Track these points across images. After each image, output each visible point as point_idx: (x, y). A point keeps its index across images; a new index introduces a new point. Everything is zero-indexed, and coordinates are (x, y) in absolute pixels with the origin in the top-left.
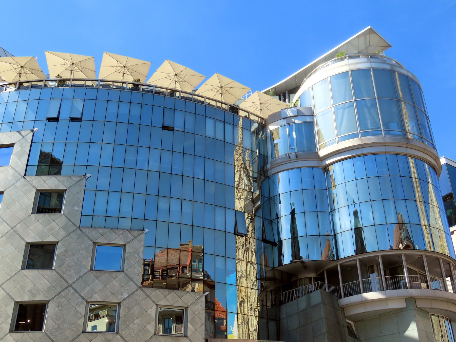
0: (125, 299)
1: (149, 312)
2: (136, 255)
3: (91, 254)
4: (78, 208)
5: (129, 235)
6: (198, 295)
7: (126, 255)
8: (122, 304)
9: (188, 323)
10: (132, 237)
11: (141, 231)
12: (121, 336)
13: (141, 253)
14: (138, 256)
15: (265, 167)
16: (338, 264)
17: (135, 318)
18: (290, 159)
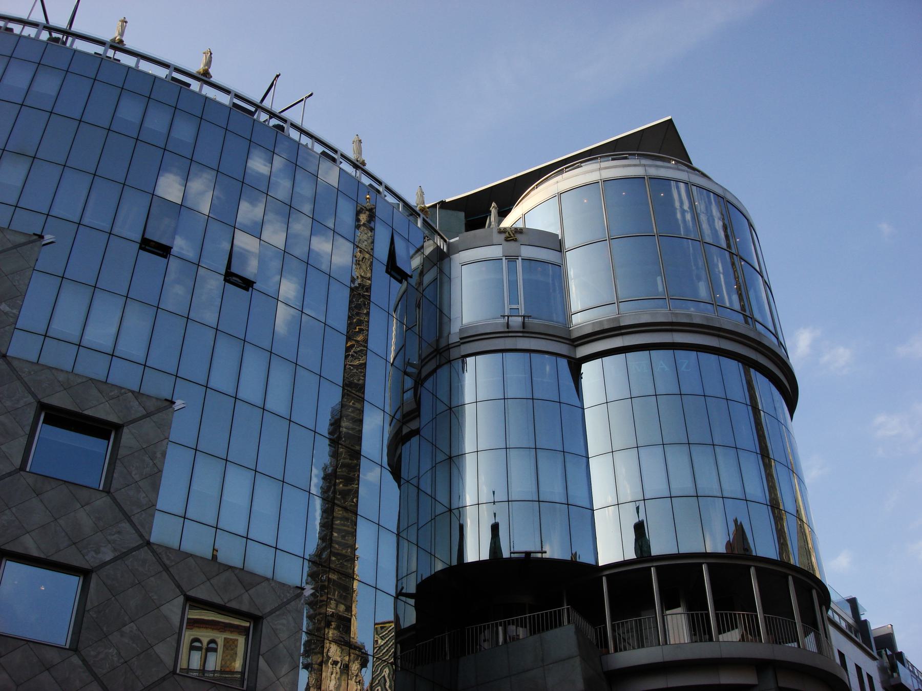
0: (104, 564)
1: (165, 609)
2: (147, 459)
3: (28, 429)
4: (10, 308)
5: (135, 404)
6: (289, 593)
7: (122, 452)
8: (94, 576)
9: (261, 658)
10: (141, 412)
14: (150, 461)
16: (604, 576)
17: (126, 618)
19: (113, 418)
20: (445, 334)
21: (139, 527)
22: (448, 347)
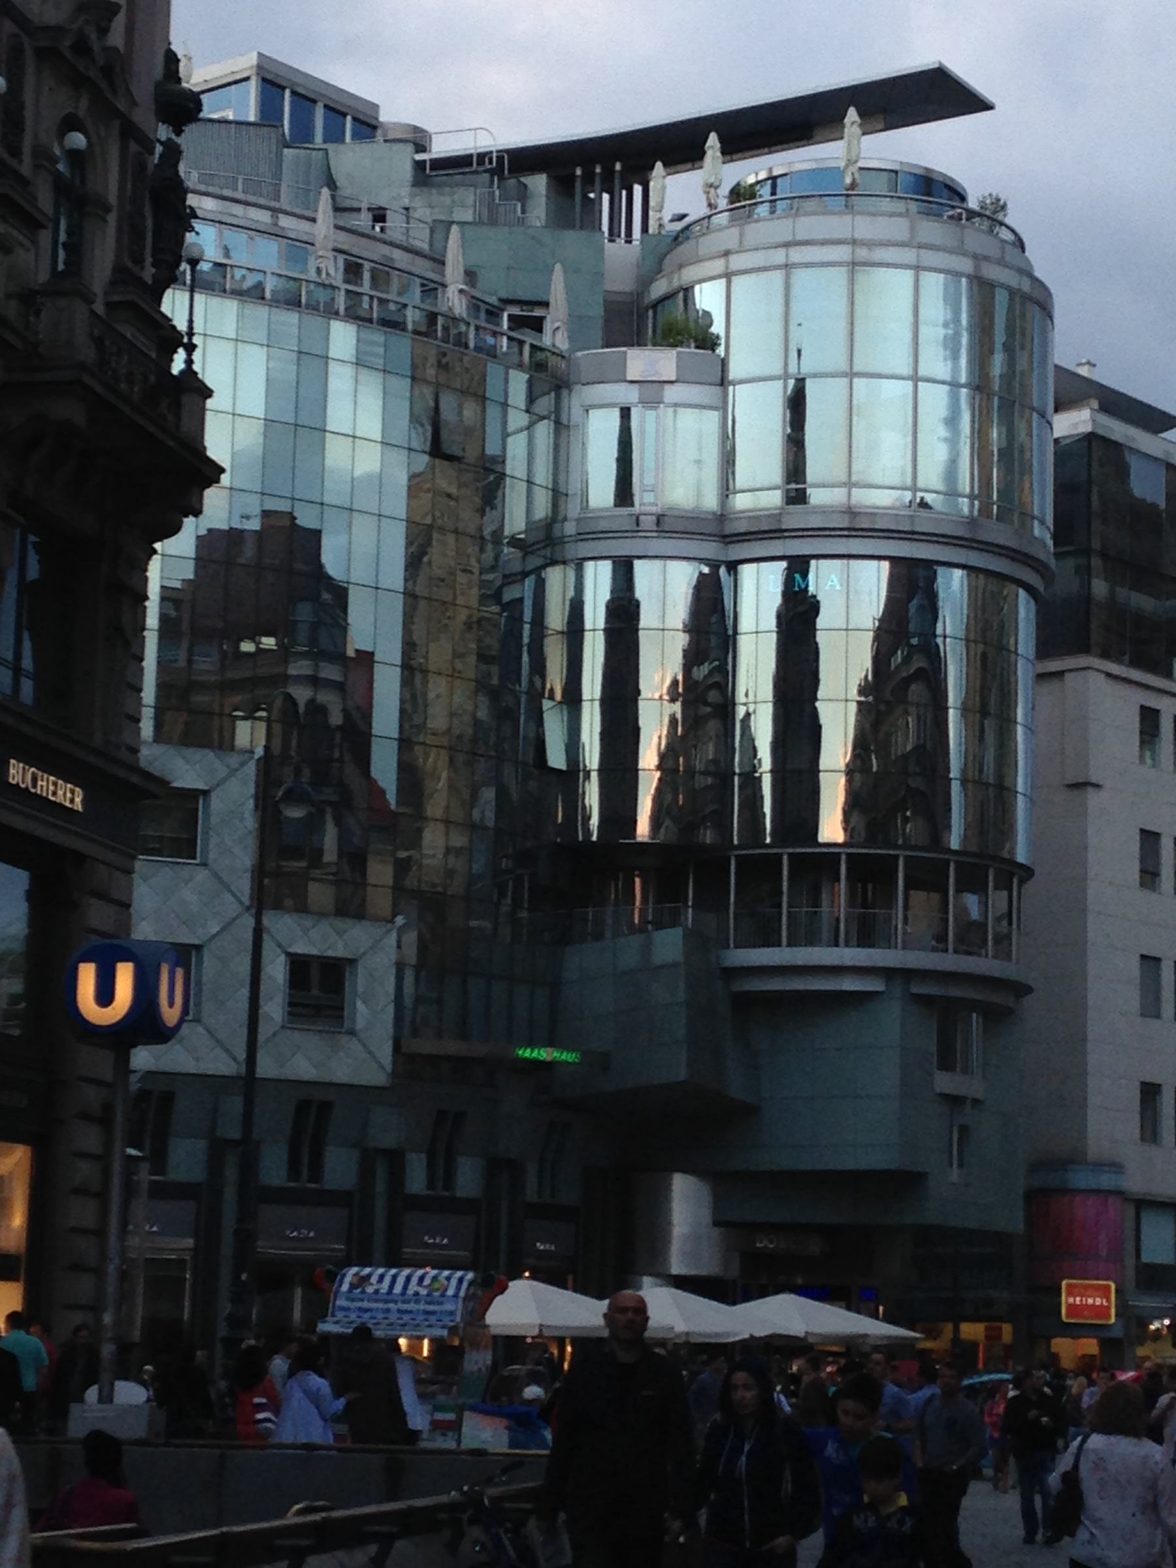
0: (215, 936)
5: (217, 764)
10: (222, 772)
11: (247, 755)
12: (209, 1032)
13: (247, 815)
15: (557, 526)
18: (638, 525)
19: (200, 786)
20: (560, 517)
21: (239, 895)
22: (562, 541)
